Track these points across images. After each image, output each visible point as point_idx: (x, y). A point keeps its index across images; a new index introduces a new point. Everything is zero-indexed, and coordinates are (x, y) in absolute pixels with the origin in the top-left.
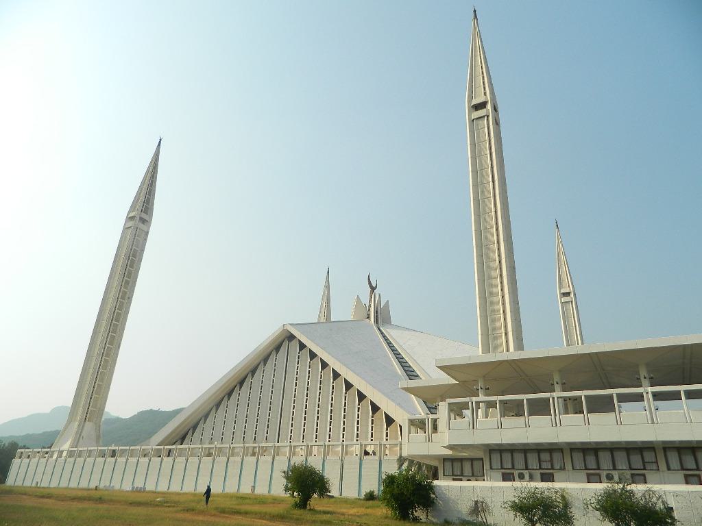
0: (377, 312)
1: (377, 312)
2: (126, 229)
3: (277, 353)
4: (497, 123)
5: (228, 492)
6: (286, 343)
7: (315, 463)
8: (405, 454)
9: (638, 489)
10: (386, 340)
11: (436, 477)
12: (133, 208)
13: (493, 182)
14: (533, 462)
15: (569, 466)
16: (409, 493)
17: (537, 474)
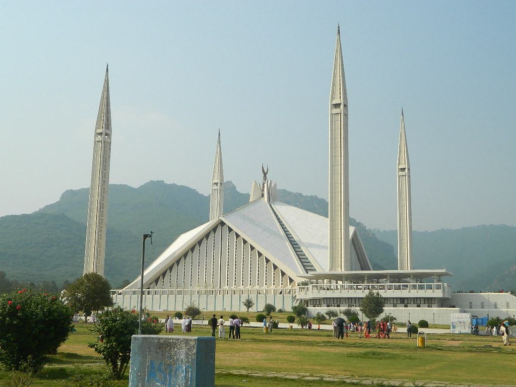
0: (269, 193)
1: (269, 193)
2: (96, 142)
3: (215, 232)
4: (346, 115)
5: (235, 311)
6: (220, 227)
7: (269, 302)
8: (297, 298)
9: (353, 308)
10: (277, 216)
11: (308, 306)
12: (98, 126)
13: (341, 156)
14: (335, 302)
15: (344, 303)
16: (300, 312)
17: (336, 305)
